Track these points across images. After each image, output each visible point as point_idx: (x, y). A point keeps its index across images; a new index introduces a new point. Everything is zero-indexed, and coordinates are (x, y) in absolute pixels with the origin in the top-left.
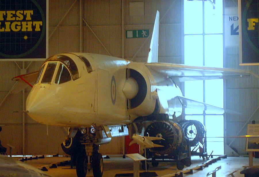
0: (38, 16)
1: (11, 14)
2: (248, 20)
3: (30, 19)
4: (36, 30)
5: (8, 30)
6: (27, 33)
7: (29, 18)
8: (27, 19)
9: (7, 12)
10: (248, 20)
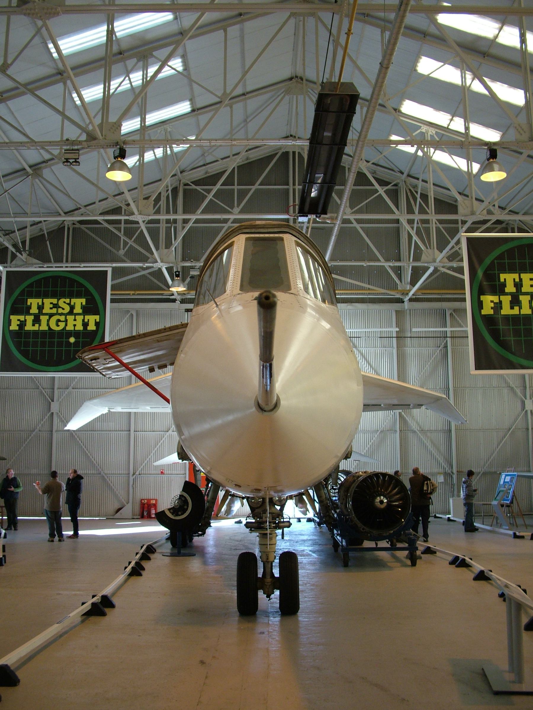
1: (51, 303)
2: (482, 298)
3: (80, 311)
4: (89, 328)
5: (44, 327)
6: (76, 334)
7: (78, 309)
8: (75, 311)
9: (45, 300)
10: (482, 298)
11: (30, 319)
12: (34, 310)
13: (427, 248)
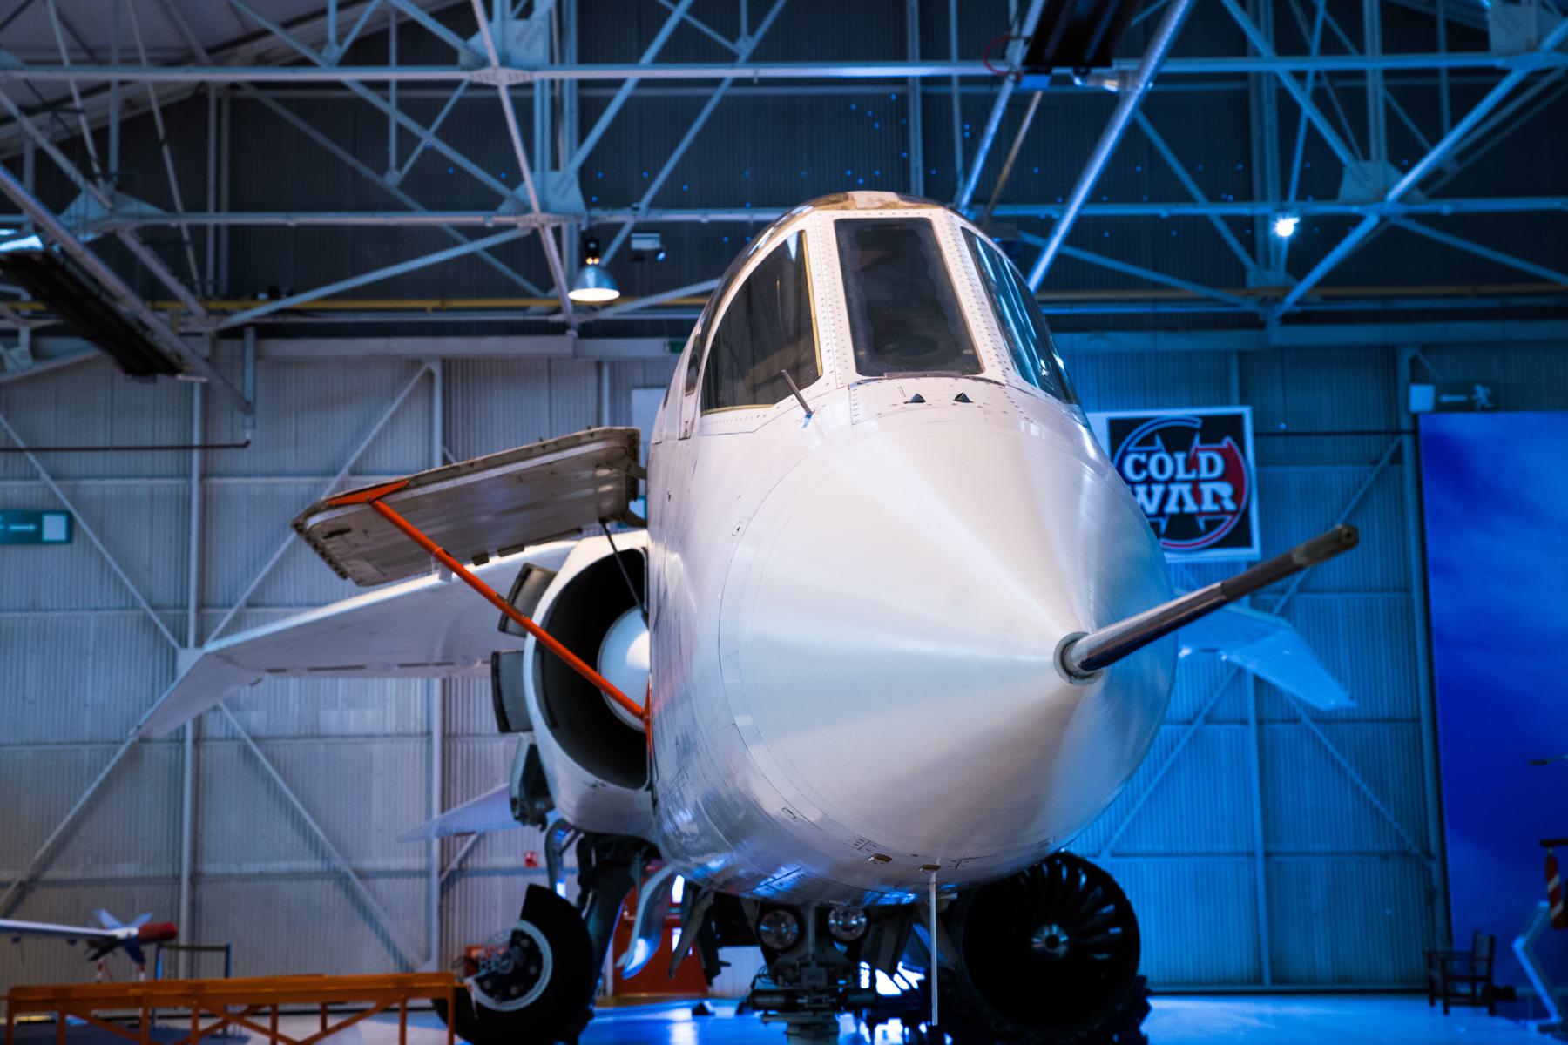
13: (1356, 158)
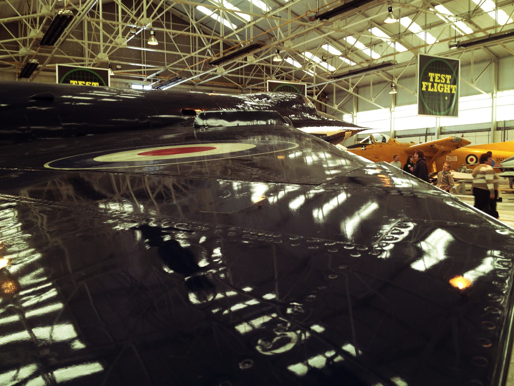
0: (454, 82)
5: (436, 90)
7: (448, 82)
11: (430, 84)
12: (431, 80)
